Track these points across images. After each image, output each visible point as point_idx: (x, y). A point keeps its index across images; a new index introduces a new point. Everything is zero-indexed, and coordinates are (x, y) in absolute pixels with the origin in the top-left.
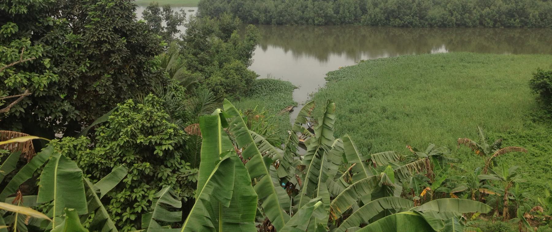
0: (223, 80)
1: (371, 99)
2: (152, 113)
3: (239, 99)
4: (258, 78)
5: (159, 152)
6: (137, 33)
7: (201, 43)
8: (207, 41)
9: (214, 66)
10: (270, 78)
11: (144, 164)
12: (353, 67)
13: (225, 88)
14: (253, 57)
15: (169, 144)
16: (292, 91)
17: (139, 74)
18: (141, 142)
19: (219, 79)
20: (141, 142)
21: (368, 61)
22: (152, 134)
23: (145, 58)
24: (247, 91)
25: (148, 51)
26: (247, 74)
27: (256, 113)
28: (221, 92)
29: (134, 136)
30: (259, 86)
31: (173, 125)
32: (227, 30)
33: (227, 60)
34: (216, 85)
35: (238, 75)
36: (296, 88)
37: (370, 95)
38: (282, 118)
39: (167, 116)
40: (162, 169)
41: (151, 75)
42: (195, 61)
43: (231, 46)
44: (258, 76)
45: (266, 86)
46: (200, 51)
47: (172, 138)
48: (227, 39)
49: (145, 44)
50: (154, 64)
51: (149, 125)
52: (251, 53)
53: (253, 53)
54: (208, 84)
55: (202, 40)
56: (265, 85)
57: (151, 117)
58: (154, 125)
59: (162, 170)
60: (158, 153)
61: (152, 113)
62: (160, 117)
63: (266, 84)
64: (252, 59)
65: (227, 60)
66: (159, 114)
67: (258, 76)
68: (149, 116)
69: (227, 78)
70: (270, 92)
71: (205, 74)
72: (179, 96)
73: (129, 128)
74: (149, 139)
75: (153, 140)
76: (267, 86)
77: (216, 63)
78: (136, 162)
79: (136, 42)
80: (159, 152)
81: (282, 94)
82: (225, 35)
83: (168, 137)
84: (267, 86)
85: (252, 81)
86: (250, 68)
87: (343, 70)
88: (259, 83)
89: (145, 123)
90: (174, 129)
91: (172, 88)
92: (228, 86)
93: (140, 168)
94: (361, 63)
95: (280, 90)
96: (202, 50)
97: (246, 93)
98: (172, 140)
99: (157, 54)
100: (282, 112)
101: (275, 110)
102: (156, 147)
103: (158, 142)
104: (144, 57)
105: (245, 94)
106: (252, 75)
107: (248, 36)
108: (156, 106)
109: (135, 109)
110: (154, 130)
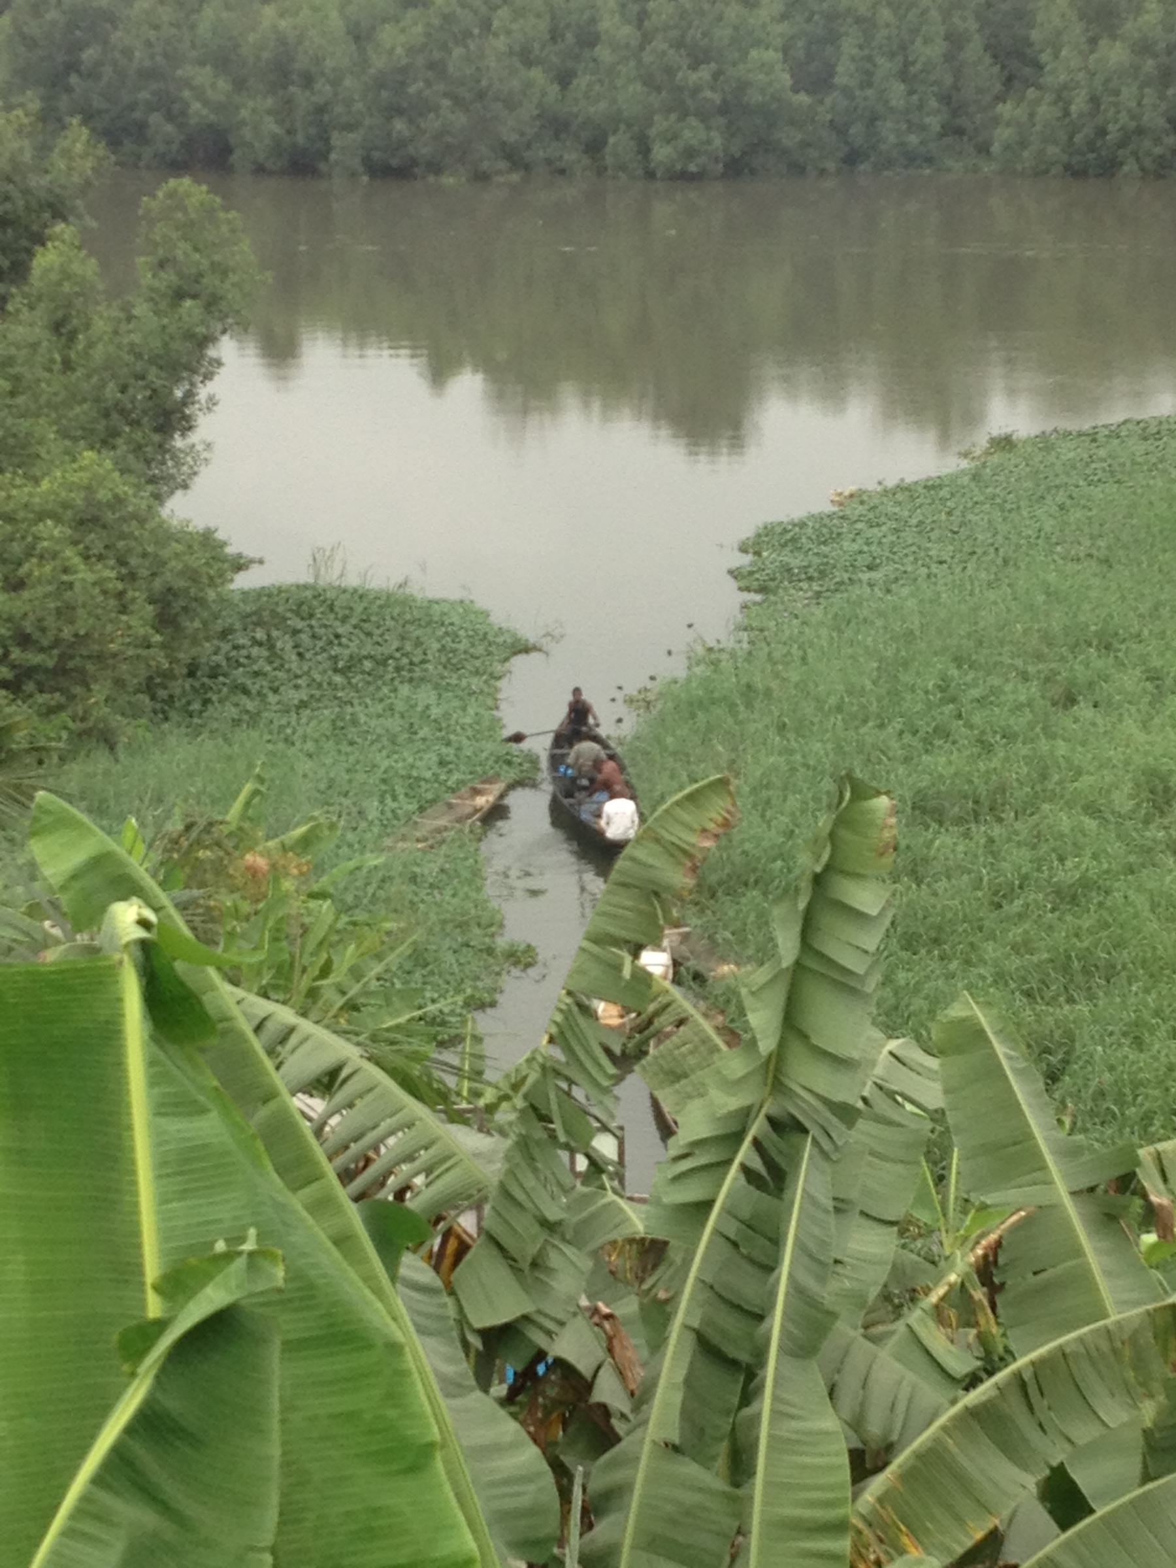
1: (1064, 721)
3: (108, 740)
4: (243, 581)
10: (330, 577)
12: (932, 486)
16: (498, 668)
21: (1044, 443)
24: (168, 675)
26: (165, 553)
27: (241, 839)
35: (100, 558)
36: (526, 649)
37: (1056, 691)
38: (430, 869)
44: (239, 565)
45: (305, 638)
52: (190, 395)
53: (203, 393)
56: (295, 632)
63: (300, 624)
64: (194, 438)
67: (239, 565)
70: (338, 679)
76: (314, 637)
81: (425, 696)
84: (314, 637)
85: (201, 601)
88: (253, 619)
94: (996, 459)
97: (162, 694)
100: (429, 823)
101: (372, 814)
105: (153, 698)
106: (198, 560)
107: (162, 265)
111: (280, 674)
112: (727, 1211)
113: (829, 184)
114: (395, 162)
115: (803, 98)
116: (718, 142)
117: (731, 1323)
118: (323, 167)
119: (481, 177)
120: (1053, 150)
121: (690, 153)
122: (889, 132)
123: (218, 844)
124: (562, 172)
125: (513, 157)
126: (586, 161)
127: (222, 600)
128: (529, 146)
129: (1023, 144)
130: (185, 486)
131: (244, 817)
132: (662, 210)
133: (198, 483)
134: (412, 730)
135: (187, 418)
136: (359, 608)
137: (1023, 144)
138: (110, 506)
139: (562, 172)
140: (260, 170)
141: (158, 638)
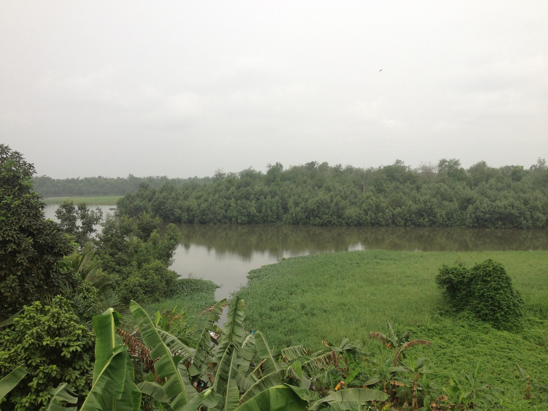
0: (142, 280)
1: (290, 296)
2: (59, 314)
3: (158, 301)
4: (179, 278)
5: (66, 353)
6: (45, 233)
7: (118, 243)
8: (125, 241)
9: (132, 266)
10: (191, 278)
11: (51, 366)
12: (274, 265)
13: (144, 289)
14: (174, 257)
15: (77, 346)
16: (214, 290)
17: (47, 275)
18: (47, 344)
19: (137, 280)
20: (47, 344)
21: (289, 259)
22: (60, 335)
23: (53, 258)
24: (167, 291)
25: (56, 251)
26: (167, 274)
27: (175, 314)
28: (140, 293)
29: (39, 337)
30: (180, 287)
31: (82, 326)
32: (147, 229)
33: (147, 261)
34: (135, 286)
35: (158, 275)
36: (218, 287)
37: (290, 293)
38: (203, 318)
39: (75, 317)
40: (70, 371)
41: (60, 276)
42: (112, 262)
43: (151, 246)
44: (179, 276)
45: (187, 286)
46: (117, 251)
47: (81, 340)
48: (146, 238)
49: (54, 244)
50: (65, 265)
51: (56, 326)
52: (172, 252)
53: (174, 252)
54: (126, 285)
55: (119, 240)
56: (186, 285)
57: (58, 318)
58: (61, 327)
59: (70, 373)
60: (65, 355)
61: (59, 314)
62: (68, 318)
63: (187, 284)
64: (173, 258)
65: (147, 261)
66: (67, 315)
67: (179, 276)
68: (56, 318)
69: (146, 279)
70: (192, 292)
71: (123, 275)
72: (91, 298)
73: (34, 330)
74: (55, 341)
75: (60, 342)
76: (189, 286)
77: (134, 263)
78: (42, 365)
79: (44, 242)
80: (67, 354)
81: (204, 294)
82: (144, 234)
83: (76, 338)
84: (189, 286)
85: (172, 281)
86: (171, 268)
87: (265, 268)
88: (180, 283)
89: (52, 324)
90: (83, 330)
91: (84, 289)
92: (147, 287)
93: (46, 371)
94: (282, 261)
95: (201, 290)
96: (120, 250)
97: (166, 294)
98: (80, 341)
99: (66, 255)
100: (203, 312)
101: (195, 311)
102: (64, 349)
103: (66, 344)
104: (52, 257)
105: (165, 294)
106: (172, 275)
107: (169, 235)
108: (64, 307)
109: (43, 312)
110: (61, 332)
111: (184, 291)
112: (224, 358)
113: (262, 225)
114: (203, 222)
115: (258, 214)
116: (247, 219)
117: (224, 374)
118: (194, 222)
119: (215, 224)
120: (291, 221)
121: (243, 221)
122: (269, 219)
123: (171, 314)
124: (226, 223)
125: (219, 221)
126: (229, 222)
127: (175, 281)
128: (221, 220)
129: (287, 220)
130: (171, 265)
131: (175, 311)
132: (239, 228)
133: (173, 265)
134: (202, 299)
135: (171, 256)
136: (195, 282)
137: (287, 220)
138: (160, 268)
139: (226, 223)
140: (185, 223)
141: (166, 286)
